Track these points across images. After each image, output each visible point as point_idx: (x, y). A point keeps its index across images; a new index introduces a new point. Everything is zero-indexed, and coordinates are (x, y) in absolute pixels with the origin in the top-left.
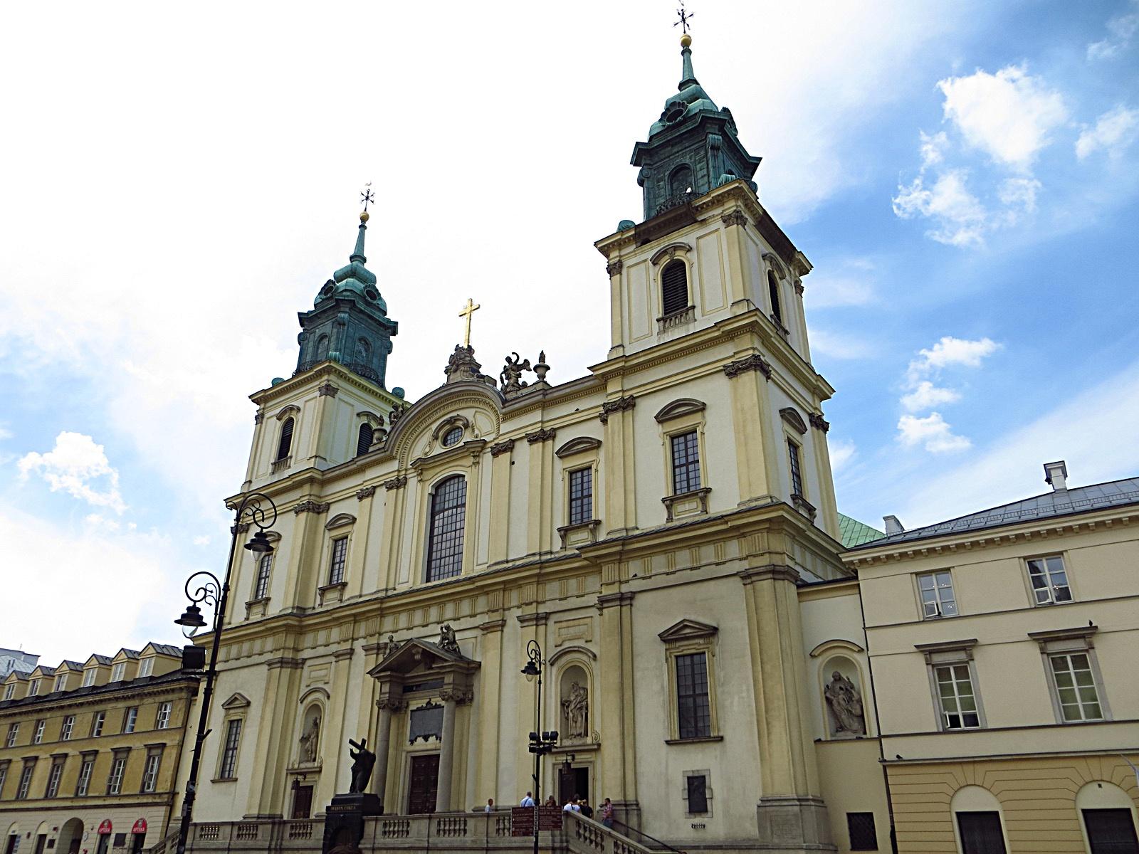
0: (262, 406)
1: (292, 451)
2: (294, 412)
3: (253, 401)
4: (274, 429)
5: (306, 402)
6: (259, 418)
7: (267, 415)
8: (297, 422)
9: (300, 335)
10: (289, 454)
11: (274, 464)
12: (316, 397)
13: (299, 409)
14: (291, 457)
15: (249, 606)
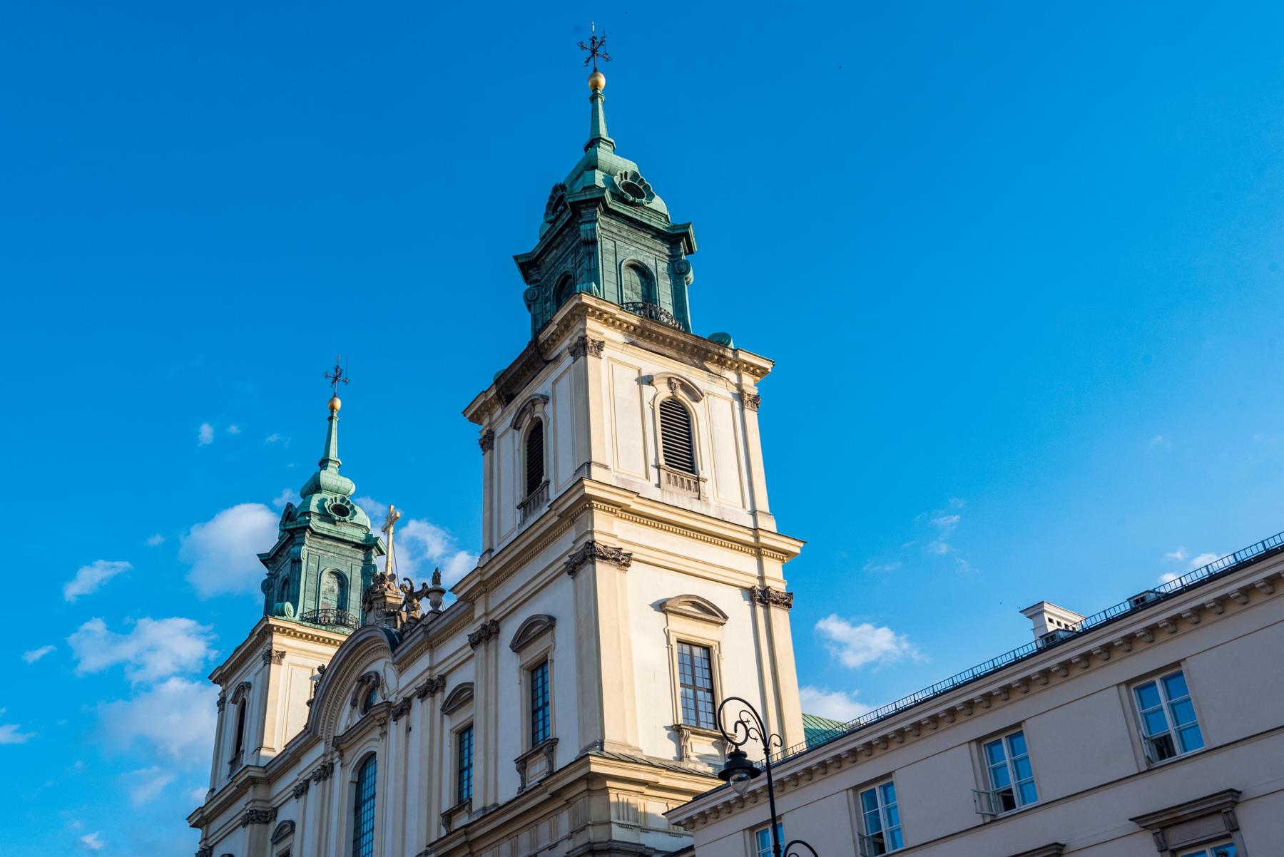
0: (486, 421)
1: (549, 472)
2: (539, 408)
3: (471, 419)
4: (511, 448)
5: (554, 383)
6: (487, 442)
7: (498, 434)
8: (548, 423)
9: (526, 293)
10: (544, 479)
11: (522, 506)
12: (569, 367)
13: (545, 399)
14: (548, 482)
15: (522, 763)
